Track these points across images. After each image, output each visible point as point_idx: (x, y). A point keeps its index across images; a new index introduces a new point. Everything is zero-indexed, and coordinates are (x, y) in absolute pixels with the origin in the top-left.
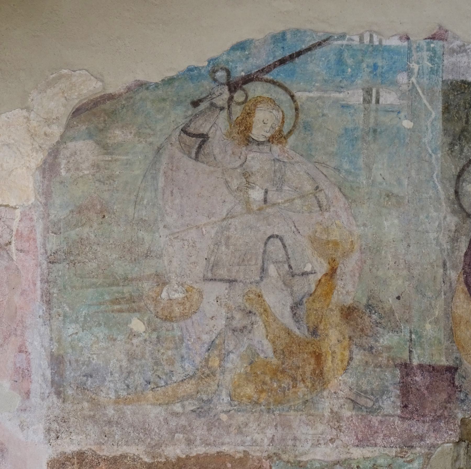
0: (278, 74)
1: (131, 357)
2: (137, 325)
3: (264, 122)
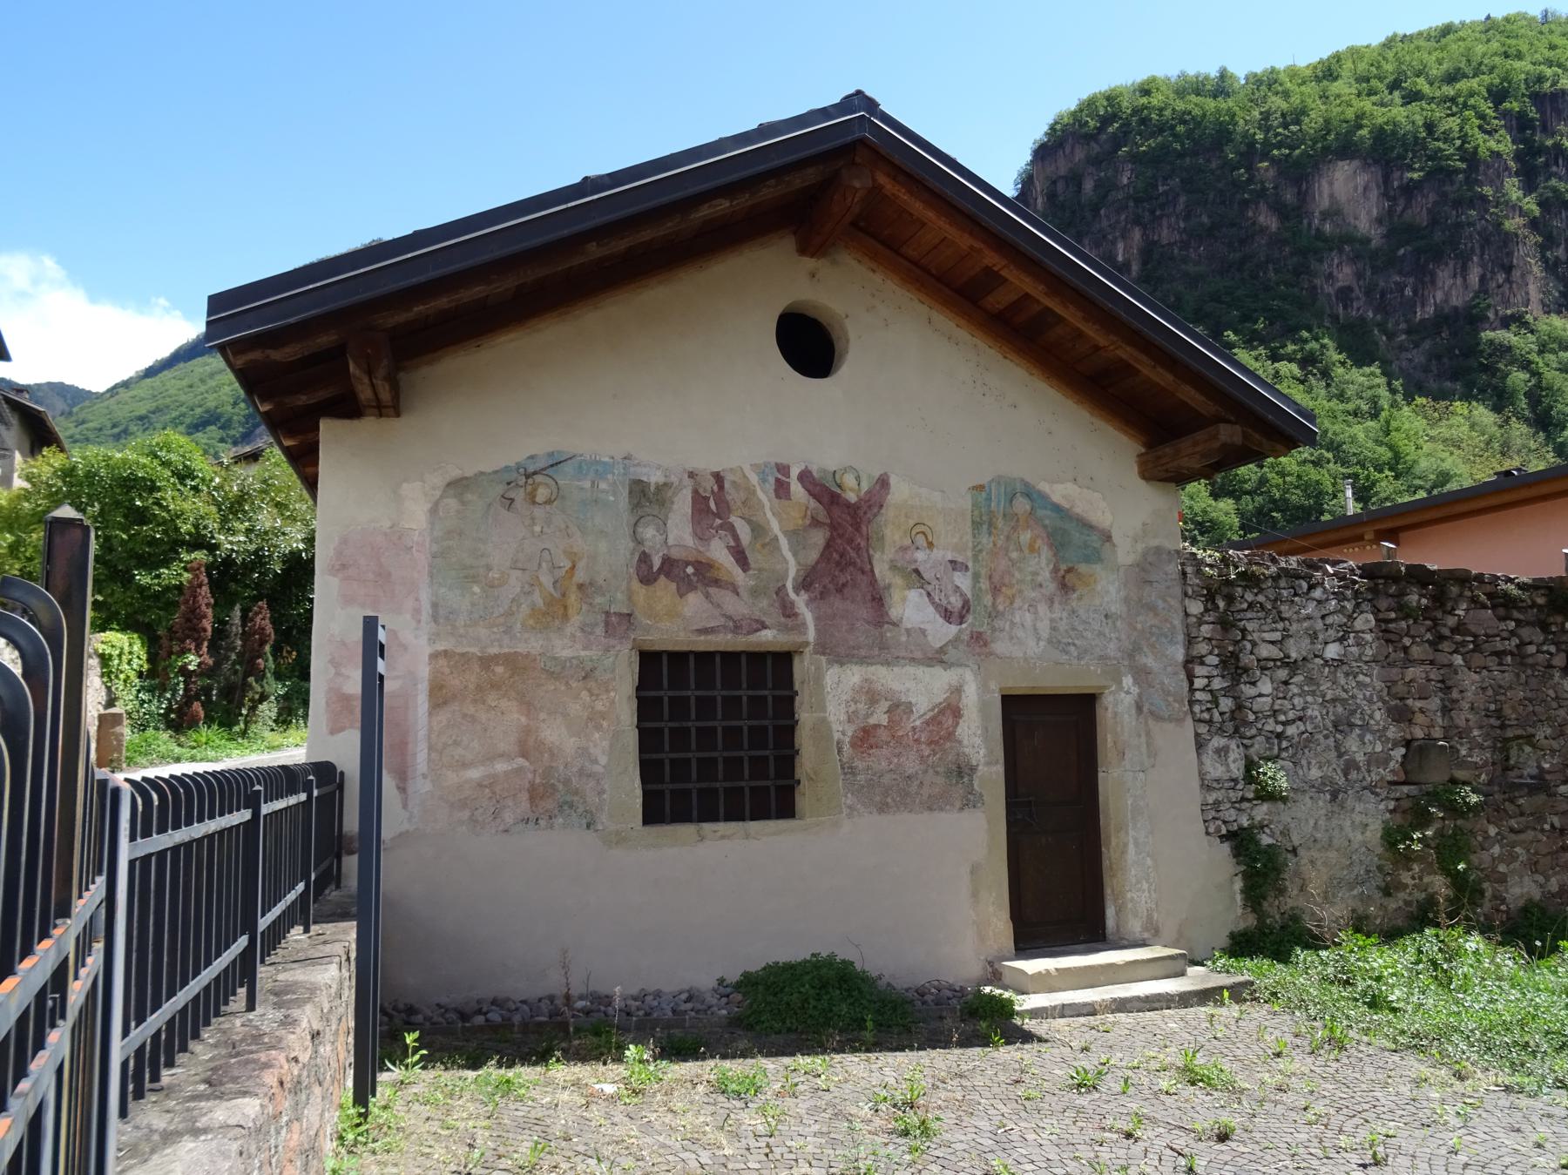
0: (550, 471)
1: (473, 605)
2: (476, 589)
3: (542, 494)
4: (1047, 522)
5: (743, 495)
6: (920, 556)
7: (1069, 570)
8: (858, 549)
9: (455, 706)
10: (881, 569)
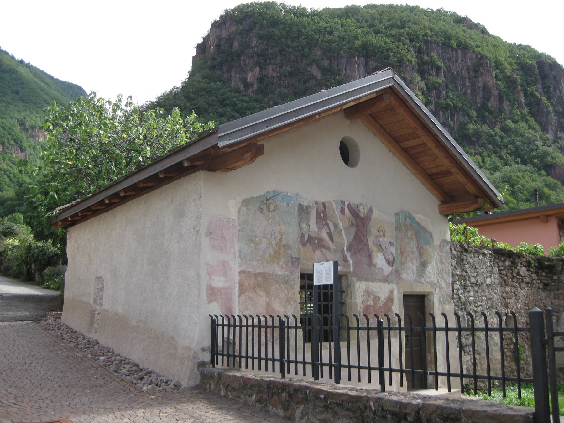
1: (252, 252)
3: (272, 207)
5: (331, 213)
6: (381, 239)
8: (364, 236)
9: (246, 294)
10: (370, 244)
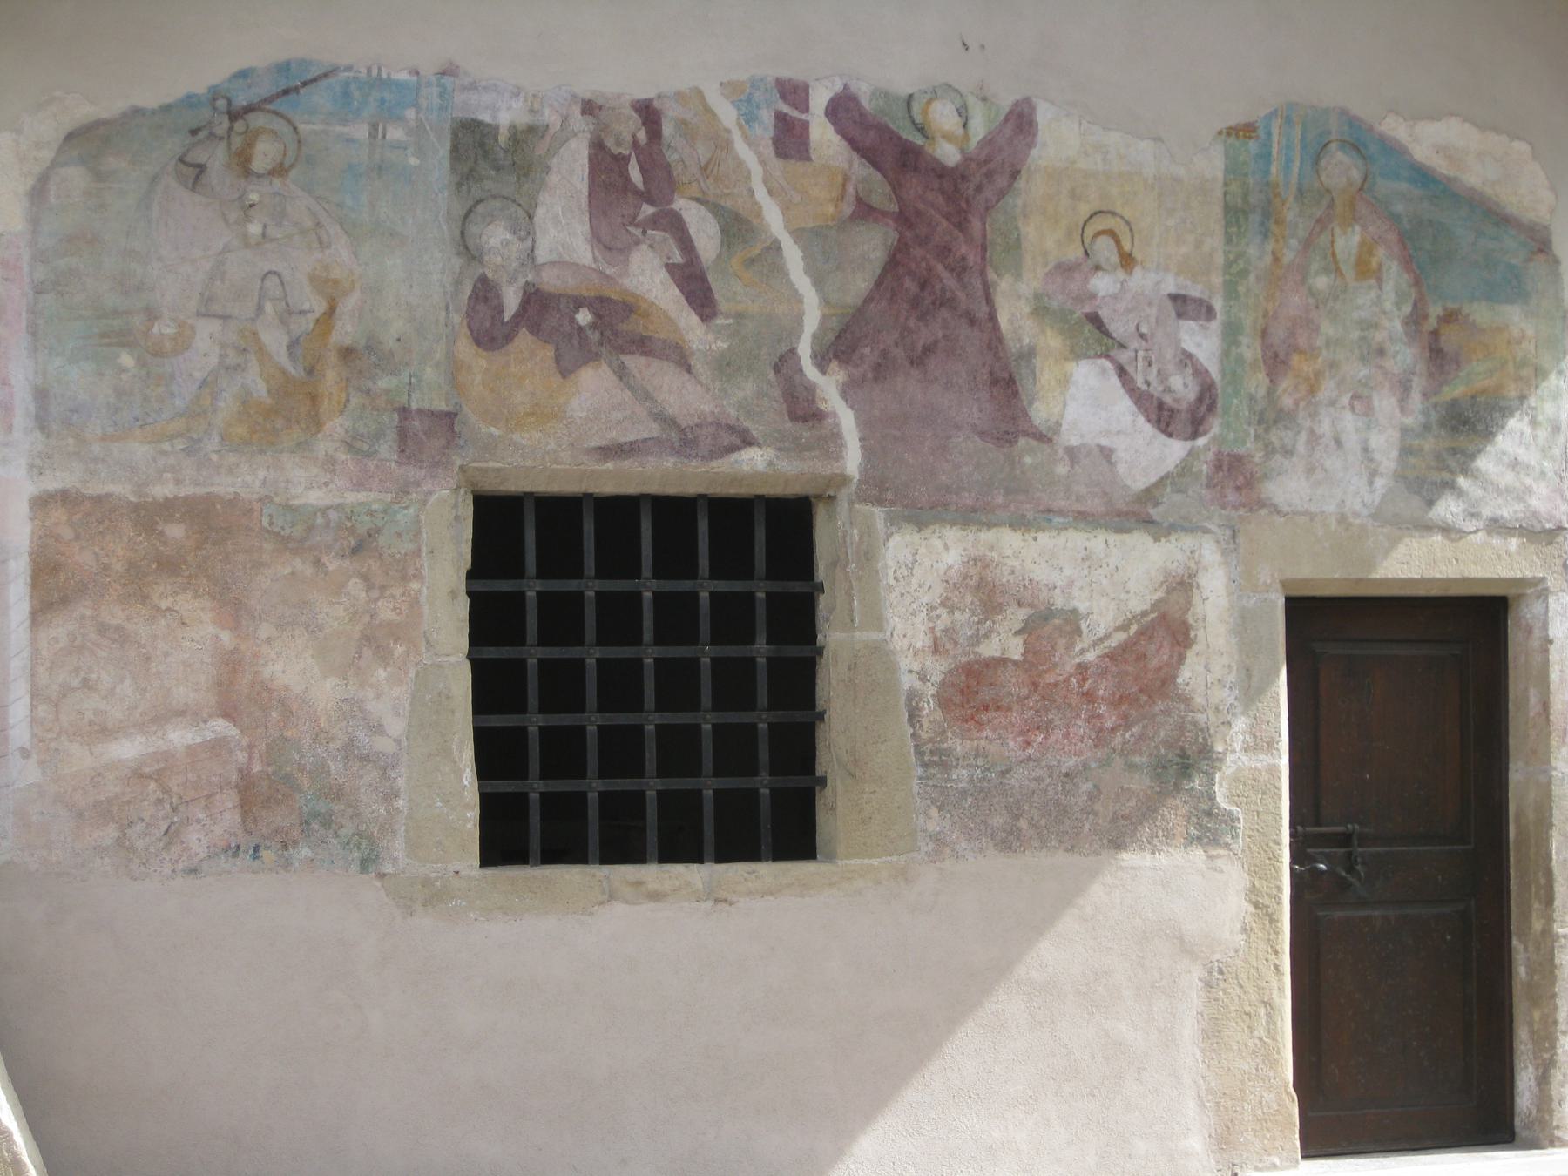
0: (281, 105)
2: (127, 360)
3: (265, 154)
4: (1399, 208)
5: (703, 152)
6: (1103, 284)
7: (1450, 317)
8: (960, 269)
9: (84, 609)
10: (1013, 312)
